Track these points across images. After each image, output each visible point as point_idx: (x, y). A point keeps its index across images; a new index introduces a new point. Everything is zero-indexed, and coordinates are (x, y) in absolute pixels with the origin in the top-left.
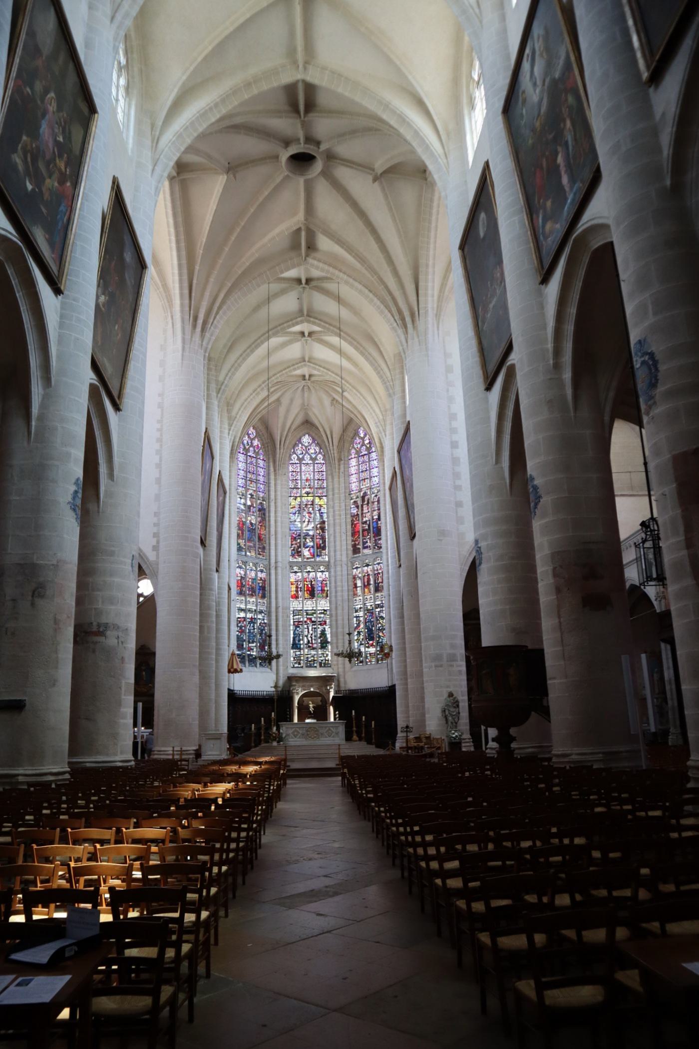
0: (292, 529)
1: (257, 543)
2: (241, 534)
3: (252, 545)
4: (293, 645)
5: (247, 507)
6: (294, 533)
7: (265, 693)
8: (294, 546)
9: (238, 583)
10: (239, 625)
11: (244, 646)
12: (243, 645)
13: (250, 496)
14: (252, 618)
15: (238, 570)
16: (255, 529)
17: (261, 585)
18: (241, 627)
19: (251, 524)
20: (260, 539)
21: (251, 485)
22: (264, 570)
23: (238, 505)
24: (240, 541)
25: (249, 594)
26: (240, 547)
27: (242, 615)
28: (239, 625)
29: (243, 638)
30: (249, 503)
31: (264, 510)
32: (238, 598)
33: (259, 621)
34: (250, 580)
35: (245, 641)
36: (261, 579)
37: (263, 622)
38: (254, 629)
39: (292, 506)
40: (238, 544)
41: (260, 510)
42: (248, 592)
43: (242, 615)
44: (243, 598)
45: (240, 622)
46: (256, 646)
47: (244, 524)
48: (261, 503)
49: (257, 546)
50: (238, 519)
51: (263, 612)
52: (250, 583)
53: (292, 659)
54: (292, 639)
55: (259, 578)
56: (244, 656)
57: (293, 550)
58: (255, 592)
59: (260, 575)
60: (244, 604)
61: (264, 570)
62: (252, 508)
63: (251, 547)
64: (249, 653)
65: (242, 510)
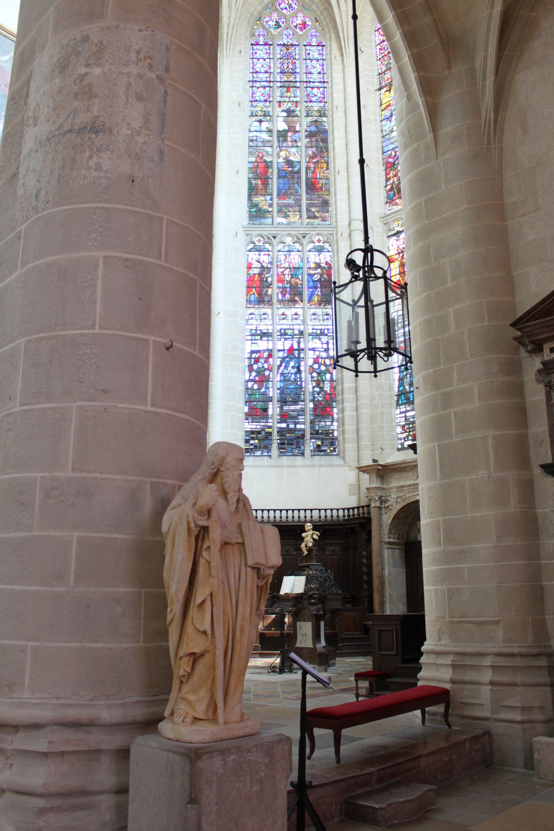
0: (386, 149)
1: (304, 196)
2: (260, 186)
3: (291, 201)
4: (399, 396)
5: (275, 134)
6: (390, 157)
7: (341, 513)
8: (391, 181)
9: (250, 279)
10: (255, 367)
11: (270, 412)
12: (265, 410)
13: (285, 114)
14: (291, 350)
15: (254, 256)
16: (299, 172)
17: (316, 277)
18: (260, 372)
19: (289, 163)
20: (312, 186)
21: (289, 94)
22: (327, 246)
23: (255, 134)
24: (258, 199)
25: (280, 302)
26: (259, 210)
27: (263, 345)
28: (255, 367)
29: (264, 394)
30: (282, 126)
31: (326, 132)
32: (252, 311)
33: (311, 356)
34: (287, 272)
35: (271, 399)
36: (318, 265)
37: (324, 355)
38: (299, 371)
39: (383, 107)
40: (252, 205)
41: (310, 135)
42: (280, 296)
43: (263, 345)
44: (269, 311)
45: (257, 361)
46: (303, 410)
47: (267, 166)
48: (316, 121)
49: (304, 203)
50: (253, 159)
51: (322, 334)
52: (288, 278)
53: (399, 430)
54: (396, 383)
55: (313, 265)
56: (270, 434)
57: (392, 189)
58: (301, 294)
59: (314, 257)
60: (269, 322)
61: (327, 246)
62: (290, 134)
63: (289, 206)
64: (284, 425)
65: (263, 142)
